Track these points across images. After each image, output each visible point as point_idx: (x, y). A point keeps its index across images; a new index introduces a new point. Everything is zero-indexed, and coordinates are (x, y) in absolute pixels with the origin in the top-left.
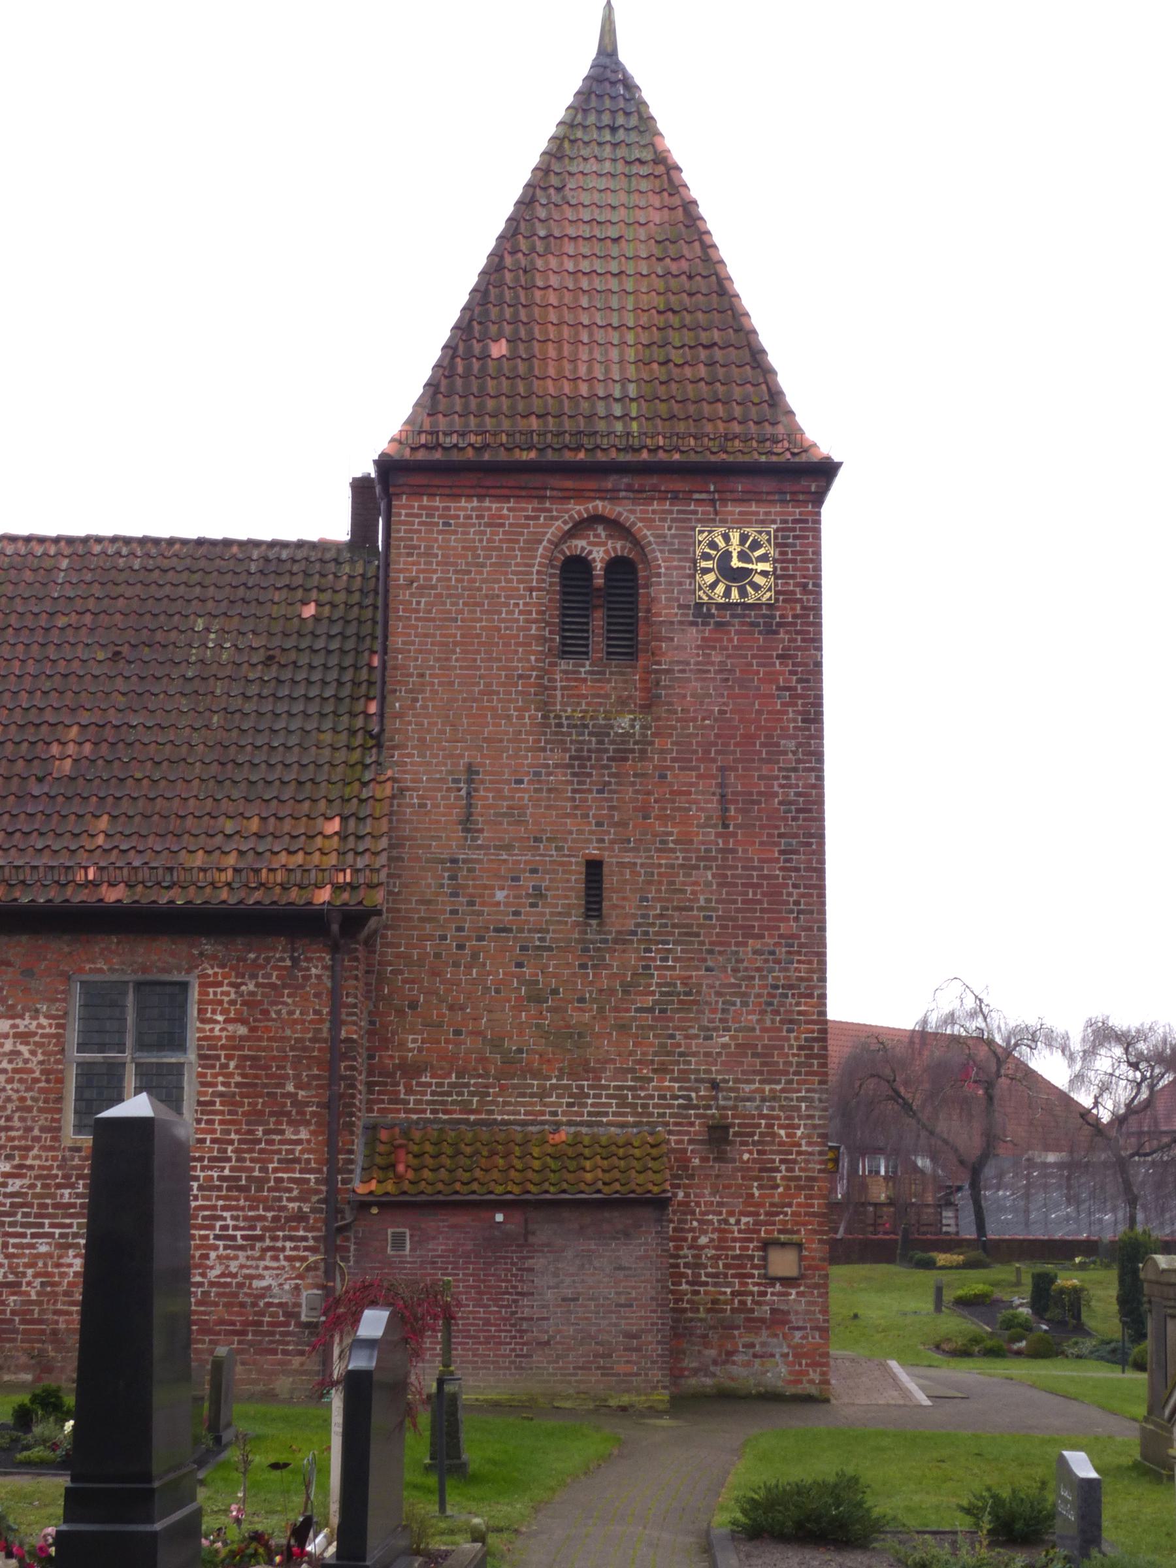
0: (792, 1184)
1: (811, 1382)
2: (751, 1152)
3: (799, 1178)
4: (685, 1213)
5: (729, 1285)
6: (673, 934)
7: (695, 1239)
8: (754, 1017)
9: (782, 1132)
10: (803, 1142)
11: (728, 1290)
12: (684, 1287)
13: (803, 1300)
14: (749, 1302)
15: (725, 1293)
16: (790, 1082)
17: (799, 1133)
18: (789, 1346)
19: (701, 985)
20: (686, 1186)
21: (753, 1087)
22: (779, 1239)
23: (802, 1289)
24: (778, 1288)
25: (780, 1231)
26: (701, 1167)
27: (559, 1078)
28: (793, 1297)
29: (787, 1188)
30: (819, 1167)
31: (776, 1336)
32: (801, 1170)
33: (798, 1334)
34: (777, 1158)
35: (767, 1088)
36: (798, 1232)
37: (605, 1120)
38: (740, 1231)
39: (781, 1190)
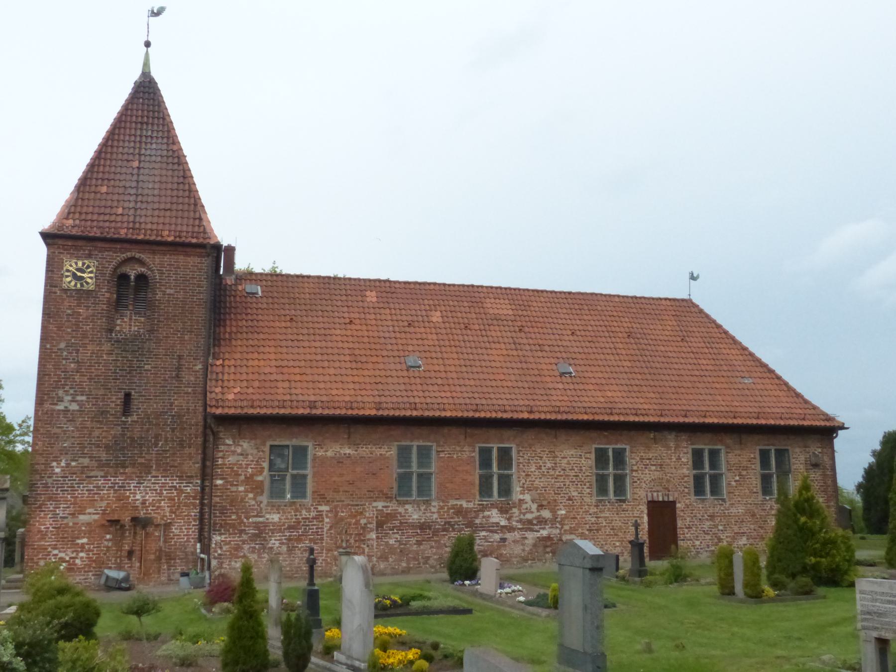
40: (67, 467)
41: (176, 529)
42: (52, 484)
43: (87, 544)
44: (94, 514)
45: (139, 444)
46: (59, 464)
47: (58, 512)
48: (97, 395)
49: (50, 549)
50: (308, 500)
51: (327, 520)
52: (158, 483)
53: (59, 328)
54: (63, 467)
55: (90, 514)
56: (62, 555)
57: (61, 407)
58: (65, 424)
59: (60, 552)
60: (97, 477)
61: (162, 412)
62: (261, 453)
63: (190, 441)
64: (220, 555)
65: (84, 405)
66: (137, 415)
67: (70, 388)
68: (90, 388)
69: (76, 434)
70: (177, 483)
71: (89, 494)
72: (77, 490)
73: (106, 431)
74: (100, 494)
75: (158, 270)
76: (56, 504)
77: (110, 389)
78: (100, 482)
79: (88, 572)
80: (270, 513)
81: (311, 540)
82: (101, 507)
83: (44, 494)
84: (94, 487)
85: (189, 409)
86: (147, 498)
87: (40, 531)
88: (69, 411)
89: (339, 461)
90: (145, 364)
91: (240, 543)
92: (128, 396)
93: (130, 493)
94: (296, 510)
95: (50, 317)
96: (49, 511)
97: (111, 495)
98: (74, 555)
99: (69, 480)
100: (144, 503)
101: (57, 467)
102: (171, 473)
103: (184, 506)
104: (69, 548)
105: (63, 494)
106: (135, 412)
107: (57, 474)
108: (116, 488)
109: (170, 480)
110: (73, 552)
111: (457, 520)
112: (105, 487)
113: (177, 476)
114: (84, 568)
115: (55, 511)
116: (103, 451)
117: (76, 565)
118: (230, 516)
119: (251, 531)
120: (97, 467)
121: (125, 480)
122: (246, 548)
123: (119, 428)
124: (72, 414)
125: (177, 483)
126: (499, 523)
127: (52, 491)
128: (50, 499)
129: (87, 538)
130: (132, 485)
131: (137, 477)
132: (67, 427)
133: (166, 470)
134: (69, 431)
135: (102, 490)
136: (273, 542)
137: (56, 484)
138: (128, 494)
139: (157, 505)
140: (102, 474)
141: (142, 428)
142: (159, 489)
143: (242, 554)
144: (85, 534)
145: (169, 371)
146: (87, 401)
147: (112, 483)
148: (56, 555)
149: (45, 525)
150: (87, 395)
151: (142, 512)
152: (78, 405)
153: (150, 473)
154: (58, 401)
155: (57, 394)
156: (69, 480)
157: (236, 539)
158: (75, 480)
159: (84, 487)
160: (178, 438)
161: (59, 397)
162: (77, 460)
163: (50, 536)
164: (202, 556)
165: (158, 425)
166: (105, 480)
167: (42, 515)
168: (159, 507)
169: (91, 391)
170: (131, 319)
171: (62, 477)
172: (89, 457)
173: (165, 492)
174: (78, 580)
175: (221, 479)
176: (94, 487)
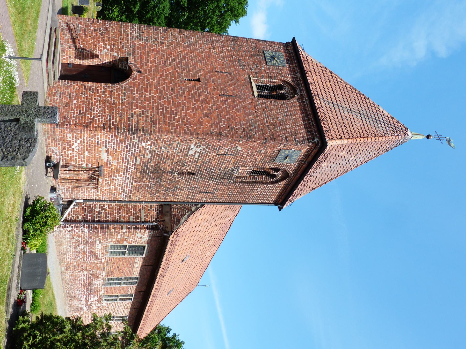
40: (145, 149)
41: (94, 191)
42: (134, 142)
43: (84, 156)
44: (108, 160)
45: (157, 178)
46: (149, 145)
47: (110, 144)
48: (197, 162)
49: (80, 139)
50: (108, 256)
51: (96, 261)
52: (127, 185)
53: (252, 147)
54: (146, 146)
55: (108, 158)
56: (76, 145)
57: (192, 146)
58: (179, 149)
59: (78, 144)
60: (136, 161)
61: (177, 187)
62: (141, 243)
63: (155, 196)
64: (75, 231)
65: (191, 157)
66: (178, 178)
67: (206, 151)
68: (203, 159)
69: (170, 153)
70: (126, 192)
71: (123, 158)
72: (127, 153)
73: (169, 166)
74: (123, 162)
75: (275, 186)
76: (117, 143)
77: (200, 167)
78: (131, 163)
79: (62, 155)
80: (102, 245)
81: (83, 257)
82: (112, 162)
83: (125, 138)
84: (128, 160)
85: (177, 196)
86: (117, 181)
87: (95, 135)
88: (189, 150)
89: (133, 264)
90: (213, 181)
91: (83, 237)
92: (193, 174)
93: (121, 175)
94: (102, 254)
95: (262, 143)
96: (112, 140)
97: (121, 167)
98: (75, 150)
99: (135, 150)
100: (113, 179)
101: (146, 144)
102: (134, 190)
103: (110, 194)
104: (81, 148)
105: (125, 147)
106: (180, 177)
107: (141, 143)
108: (126, 169)
109: (129, 189)
110: (79, 150)
111: (93, 291)
112: (128, 164)
113: (131, 192)
114: (65, 154)
115: (111, 142)
116: (155, 164)
117: (68, 150)
118: (101, 234)
119: (90, 240)
120: (143, 161)
121: (132, 172)
122: (79, 239)
123: (171, 171)
124: (186, 152)
125: (126, 192)
126: (90, 299)
127: (128, 141)
128: (121, 141)
129: (89, 156)
130: (127, 175)
131: (133, 178)
132: (176, 149)
133: (136, 188)
134: (173, 150)
135: (125, 163)
136: (83, 247)
137: (133, 144)
138: (121, 173)
139: (112, 184)
140: (138, 163)
141: (168, 179)
142: (123, 185)
143: (74, 237)
144: (92, 155)
145: (205, 189)
146: (193, 158)
147: (130, 167)
148: (76, 142)
149: (101, 138)
150: (198, 158)
151: (107, 179)
152: (192, 154)
153: (135, 182)
154: (198, 145)
155: (203, 145)
156: (135, 150)
157: (85, 236)
158: (135, 152)
159: (129, 156)
160: (158, 192)
161: (200, 146)
162: (150, 153)
163: (91, 139)
164: (74, 203)
165: (169, 185)
166: (133, 165)
167: (108, 136)
168: (110, 185)
169: (200, 159)
170: (247, 170)
171: (138, 147)
172: (151, 159)
173: (121, 187)
174: (55, 151)
175: (126, 232)
176: (128, 160)
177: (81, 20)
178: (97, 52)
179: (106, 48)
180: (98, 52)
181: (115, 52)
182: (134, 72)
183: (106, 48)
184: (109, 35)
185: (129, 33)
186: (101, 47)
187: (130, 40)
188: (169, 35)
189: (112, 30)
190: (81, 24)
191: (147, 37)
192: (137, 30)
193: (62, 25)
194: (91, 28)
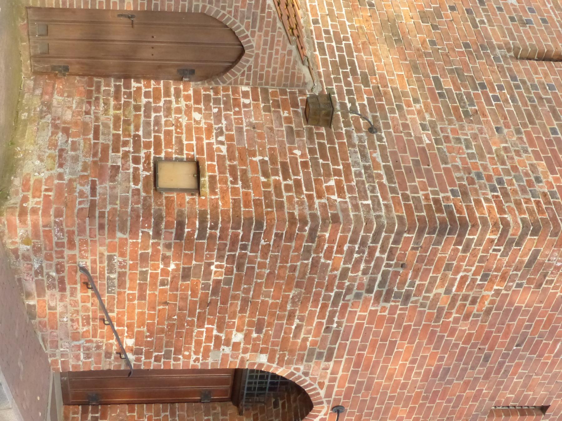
0: (272, 189)
1: (25, 199)
2: (302, 156)
3: (279, 194)
4: (225, 103)
5: (147, 134)
6: (525, 104)
7: (199, 110)
8: (459, 163)
9: (332, 183)
10: (324, 201)
11: (141, 133)
12: (144, 100)
13: (130, 194)
14: (127, 149)
15: (137, 129)
16: (393, 190)
17: (335, 197)
18: (70, 180)
19: (479, 123)
20: (256, 107)
21: (379, 160)
22: (204, 176)
23: (143, 194)
24: (143, 174)
25: (212, 179)
26: (279, 117)
27: (351, 27)
28: (133, 186)
29: (266, 185)
30: (296, 213)
31: (85, 169)
32: (290, 199)
33: (87, 189)
34: (301, 177)
35: (382, 172)
36: (213, 191)
37: (317, 53)
38: (210, 145)
39: (263, 179)
177: (119, 235)
178: (189, 357)
179: (227, 342)
180: (194, 357)
181: (263, 351)
182: (316, 408)
183: (227, 342)
184: (247, 291)
185: (338, 273)
186: (208, 339)
187: (335, 304)
188: (521, 262)
189: (262, 266)
190: (122, 255)
191: (412, 284)
192: (377, 254)
193: (36, 266)
194: (167, 264)
